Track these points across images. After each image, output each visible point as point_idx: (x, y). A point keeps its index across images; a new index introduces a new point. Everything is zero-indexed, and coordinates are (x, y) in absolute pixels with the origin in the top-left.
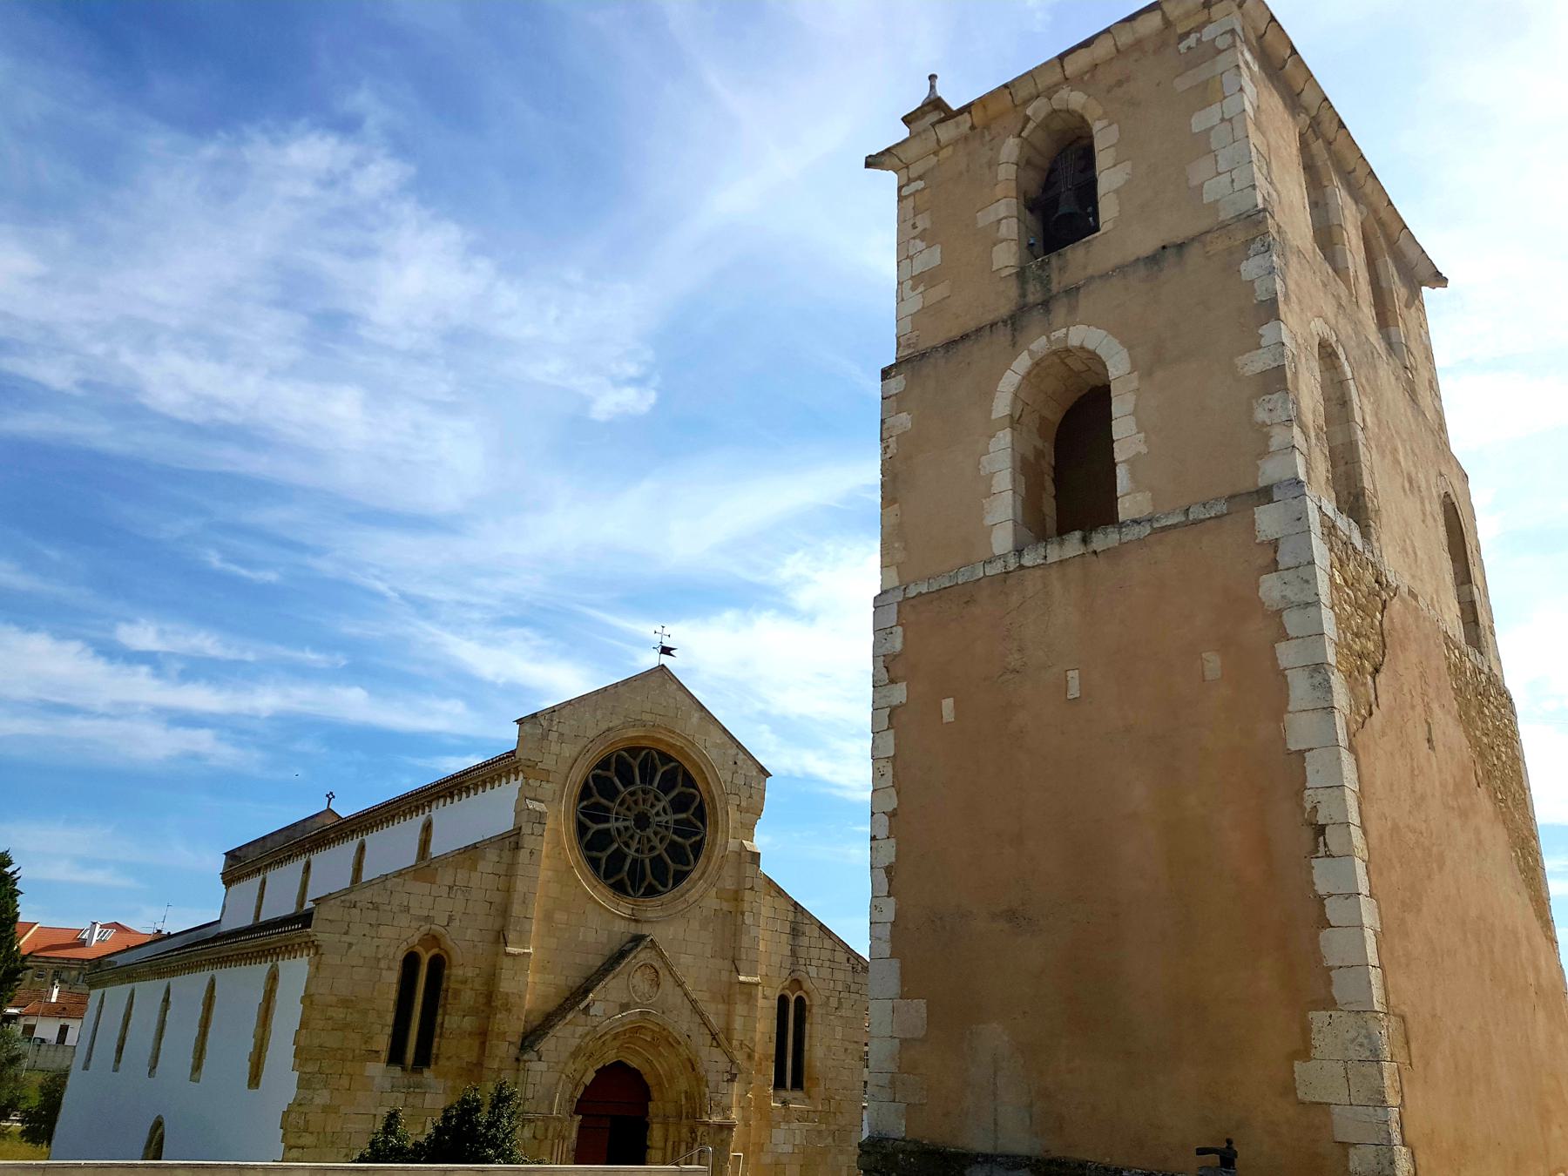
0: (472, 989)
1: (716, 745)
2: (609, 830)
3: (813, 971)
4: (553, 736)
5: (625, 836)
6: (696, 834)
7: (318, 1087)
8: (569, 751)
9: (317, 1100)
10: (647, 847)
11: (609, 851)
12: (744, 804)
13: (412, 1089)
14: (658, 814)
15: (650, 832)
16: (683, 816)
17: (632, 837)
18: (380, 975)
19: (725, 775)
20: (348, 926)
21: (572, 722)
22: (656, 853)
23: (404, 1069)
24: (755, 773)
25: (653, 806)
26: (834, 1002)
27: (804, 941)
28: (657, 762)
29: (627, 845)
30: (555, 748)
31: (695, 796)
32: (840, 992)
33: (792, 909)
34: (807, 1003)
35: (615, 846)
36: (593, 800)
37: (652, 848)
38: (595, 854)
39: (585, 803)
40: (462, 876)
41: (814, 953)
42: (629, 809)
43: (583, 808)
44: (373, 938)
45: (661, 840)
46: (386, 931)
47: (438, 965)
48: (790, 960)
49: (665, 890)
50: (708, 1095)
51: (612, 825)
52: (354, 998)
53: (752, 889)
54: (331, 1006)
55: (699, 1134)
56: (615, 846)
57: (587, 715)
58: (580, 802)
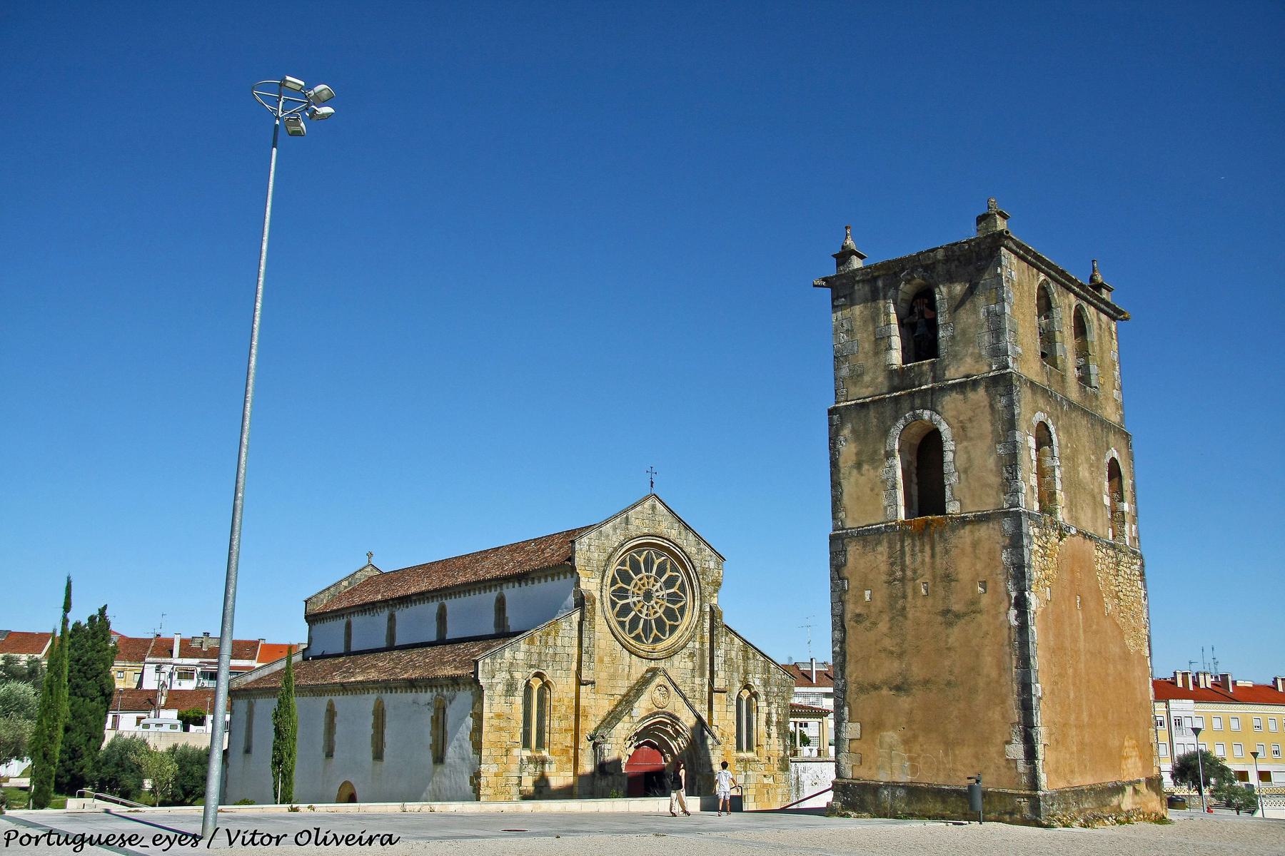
6: (681, 601)
10: (652, 611)
14: (657, 591)
15: (653, 602)
16: (672, 590)
17: (642, 607)
22: (657, 615)
25: (654, 585)
29: (641, 612)
35: (633, 613)
36: (618, 586)
38: (622, 619)
39: (613, 588)
43: (614, 591)
55: (697, 780)
56: (633, 613)
58: (611, 587)
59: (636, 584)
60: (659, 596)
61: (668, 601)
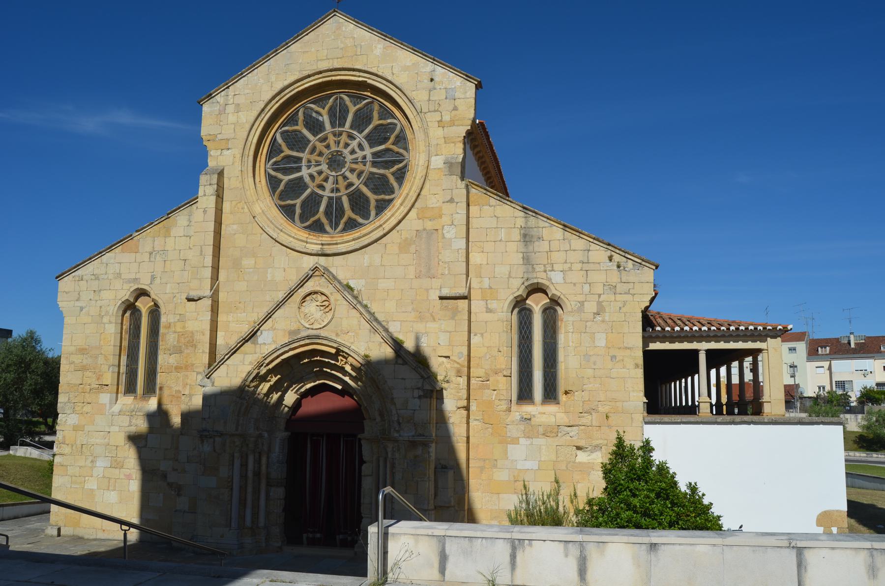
0: (175, 332)
1: (406, 68)
2: (301, 178)
4: (230, 109)
6: (400, 161)
7: (68, 412)
12: (447, 118)
13: (134, 413)
17: (326, 180)
18: (105, 328)
19: (420, 97)
20: (79, 294)
21: (247, 91)
23: (136, 397)
25: (347, 145)
26: (591, 307)
27: (544, 246)
30: (232, 118)
31: (396, 125)
32: (600, 295)
35: (308, 191)
37: (350, 185)
39: (274, 160)
41: (557, 257)
42: (321, 154)
44: (96, 301)
45: (359, 176)
46: (106, 295)
48: (522, 269)
50: (394, 412)
52: (87, 347)
54: (72, 354)
57: (262, 81)
60: (357, 159)
61: (374, 164)
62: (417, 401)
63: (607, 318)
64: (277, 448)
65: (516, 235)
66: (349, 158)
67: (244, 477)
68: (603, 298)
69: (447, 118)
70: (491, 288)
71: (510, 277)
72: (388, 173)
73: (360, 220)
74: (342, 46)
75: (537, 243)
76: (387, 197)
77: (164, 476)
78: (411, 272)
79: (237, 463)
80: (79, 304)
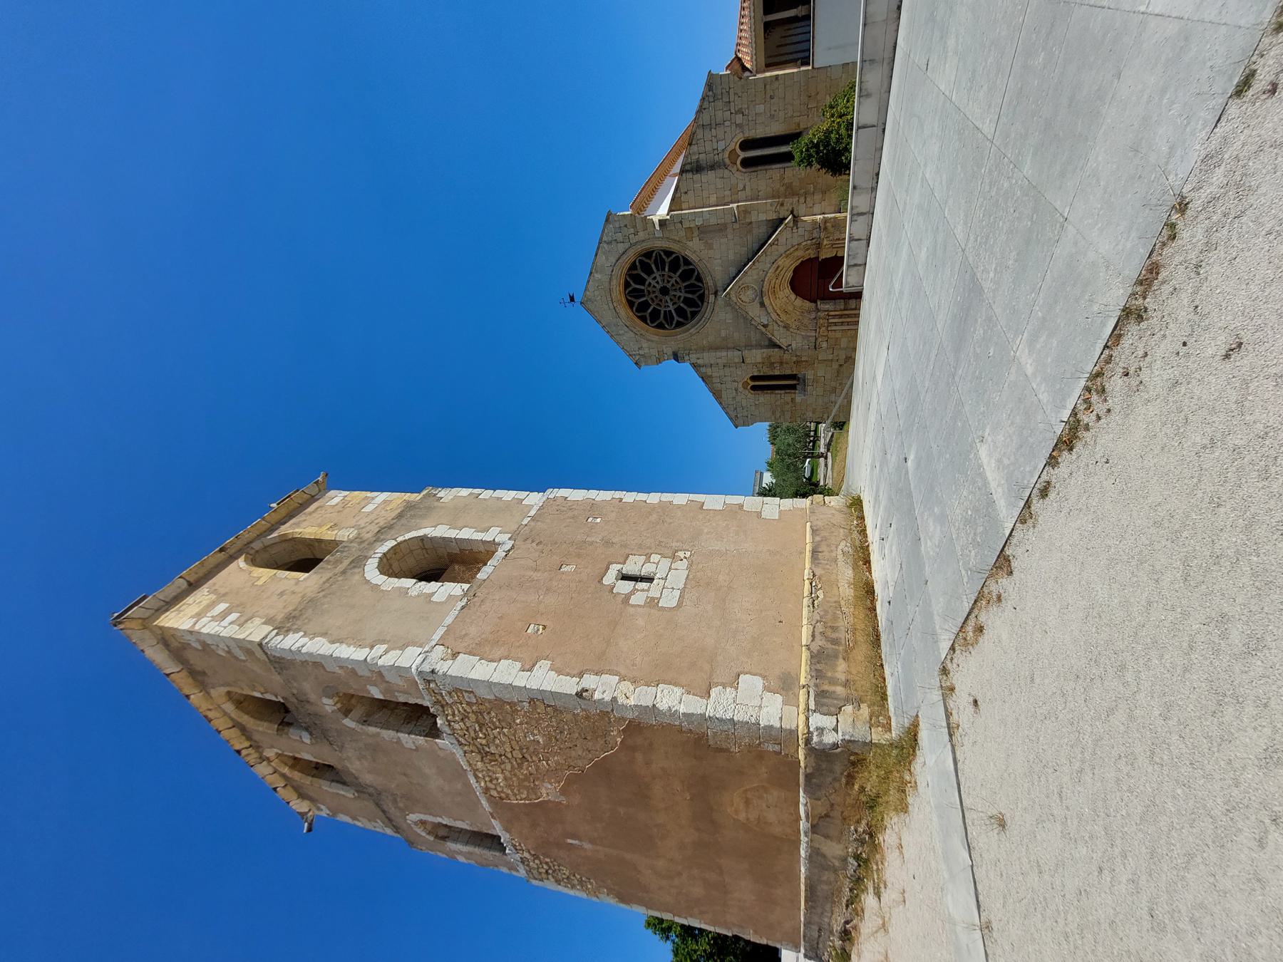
1: (607, 259)
2: (675, 310)
3: (721, 145)
4: (641, 352)
5: (676, 300)
8: (645, 345)
9: (811, 415)
10: (676, 300)
11: (685, 307)
12: (632, 230)
14: (658, 282)
15: (669, 286)
17: (675, 296)
22: (678, 280)
24: (611, 226)
25: (654, 287)
26: (739, 118)
28: (630, 289)
29: (680, 297)
30: (646, 351)
32: (731, 113)
33: (684, 175)
34: (743, 139)
35: (681, 305)
38: (689, 315)
40: (715, 380)
42: (661, 300)
47: (753, 378)
49: (699, 309)
50: (805, 243)
51: (672, 308)
53: (681, 222)
59: (658, 304)
61: (663, 269)
62: (800, 229)
63: (746, 106)
64: (827, 307)
65: (697, 177)
66: (661, 284)
67: (842, 323)
68: (733, 111)
69: (632, 230)
70: (731, 190)
71: (723, 178)
72: (667, 260)
73: (696, 273)
74: (600, 297)
75: (701, 162)
76: (681, 259)
77: (841, 365)
78: (724, 240)
79: (834, 328)
80: (749, 416)
